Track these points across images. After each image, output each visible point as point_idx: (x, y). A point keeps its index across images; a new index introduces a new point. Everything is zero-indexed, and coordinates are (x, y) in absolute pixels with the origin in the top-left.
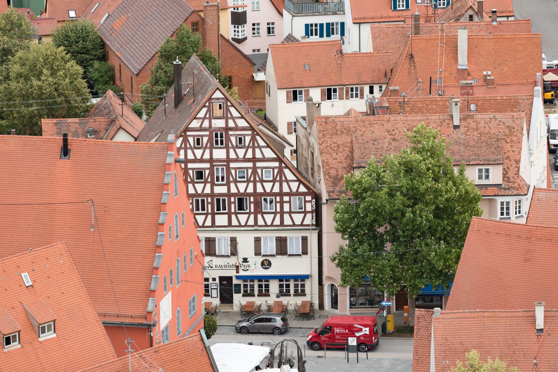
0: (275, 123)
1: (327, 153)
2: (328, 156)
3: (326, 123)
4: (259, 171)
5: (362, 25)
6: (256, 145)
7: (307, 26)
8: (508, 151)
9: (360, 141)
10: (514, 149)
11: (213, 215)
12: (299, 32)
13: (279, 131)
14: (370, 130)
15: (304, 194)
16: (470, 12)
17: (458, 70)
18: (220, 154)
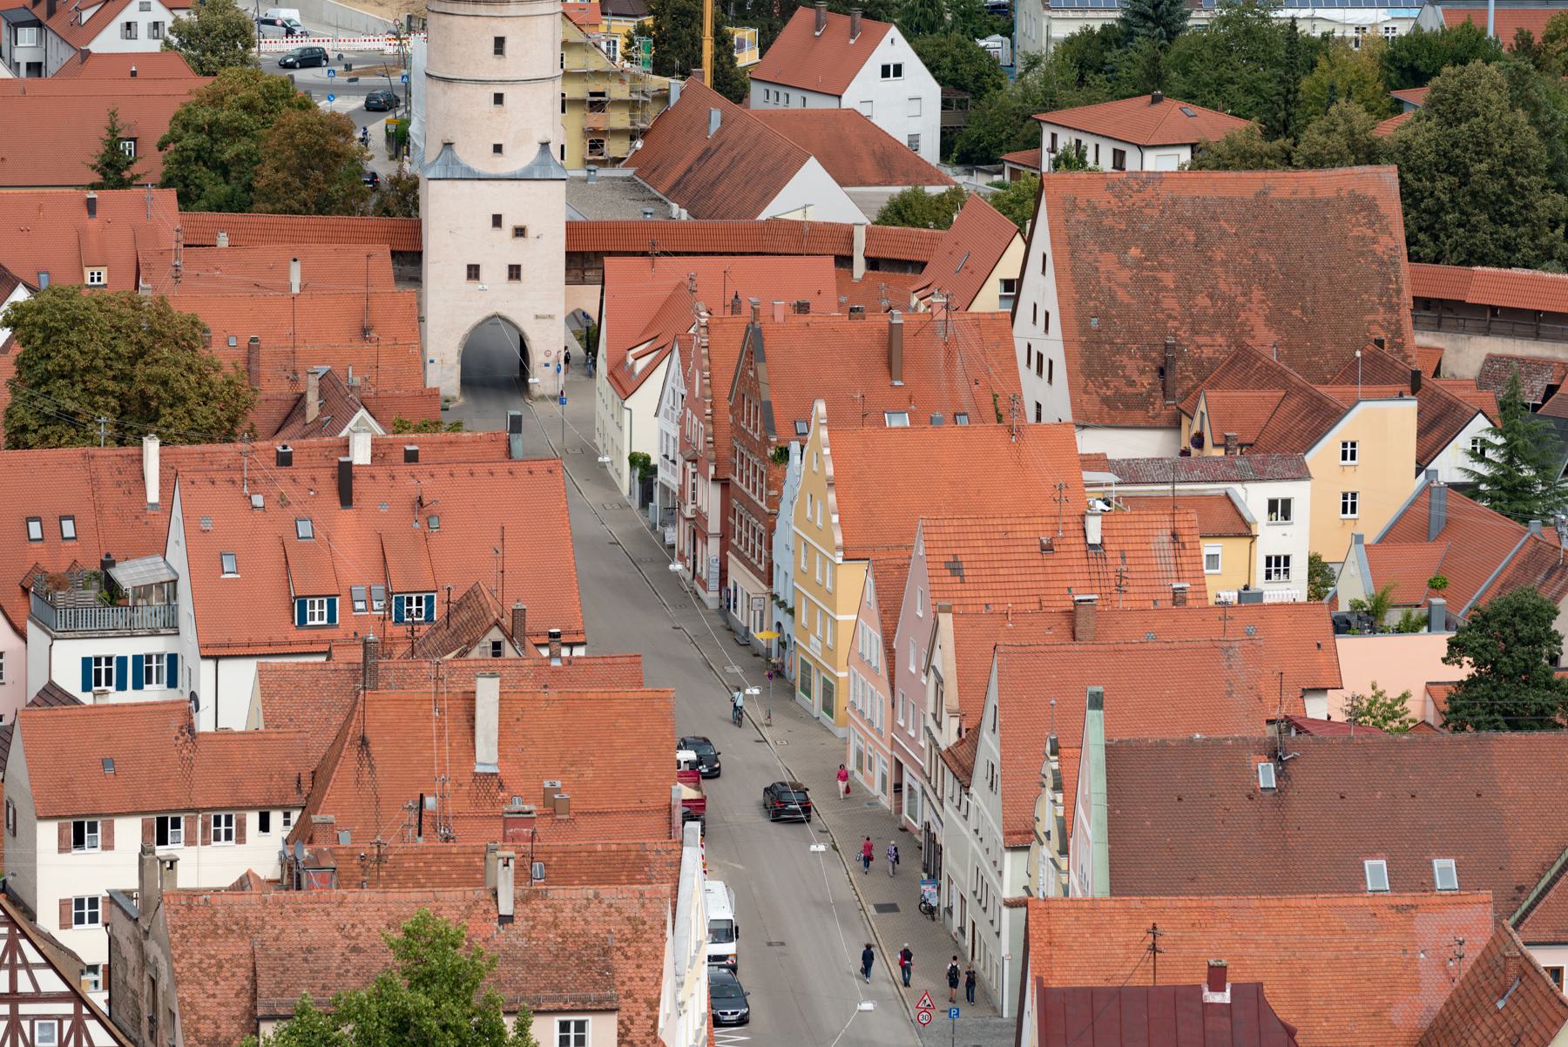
0: (27, 900)
1: (191, 983)
2: (195, 989)
3: (190, 907)
4: (25, 1025)
5: (221, 663)
6: (19, 961)
7: (86, 662)
8: (631, 979)
9: (273, 951)
10: (644, 972)
12: (69, 679)
13: (39, 921)
14: (296, 927)
16: (496, 635)
17: (476, 774)
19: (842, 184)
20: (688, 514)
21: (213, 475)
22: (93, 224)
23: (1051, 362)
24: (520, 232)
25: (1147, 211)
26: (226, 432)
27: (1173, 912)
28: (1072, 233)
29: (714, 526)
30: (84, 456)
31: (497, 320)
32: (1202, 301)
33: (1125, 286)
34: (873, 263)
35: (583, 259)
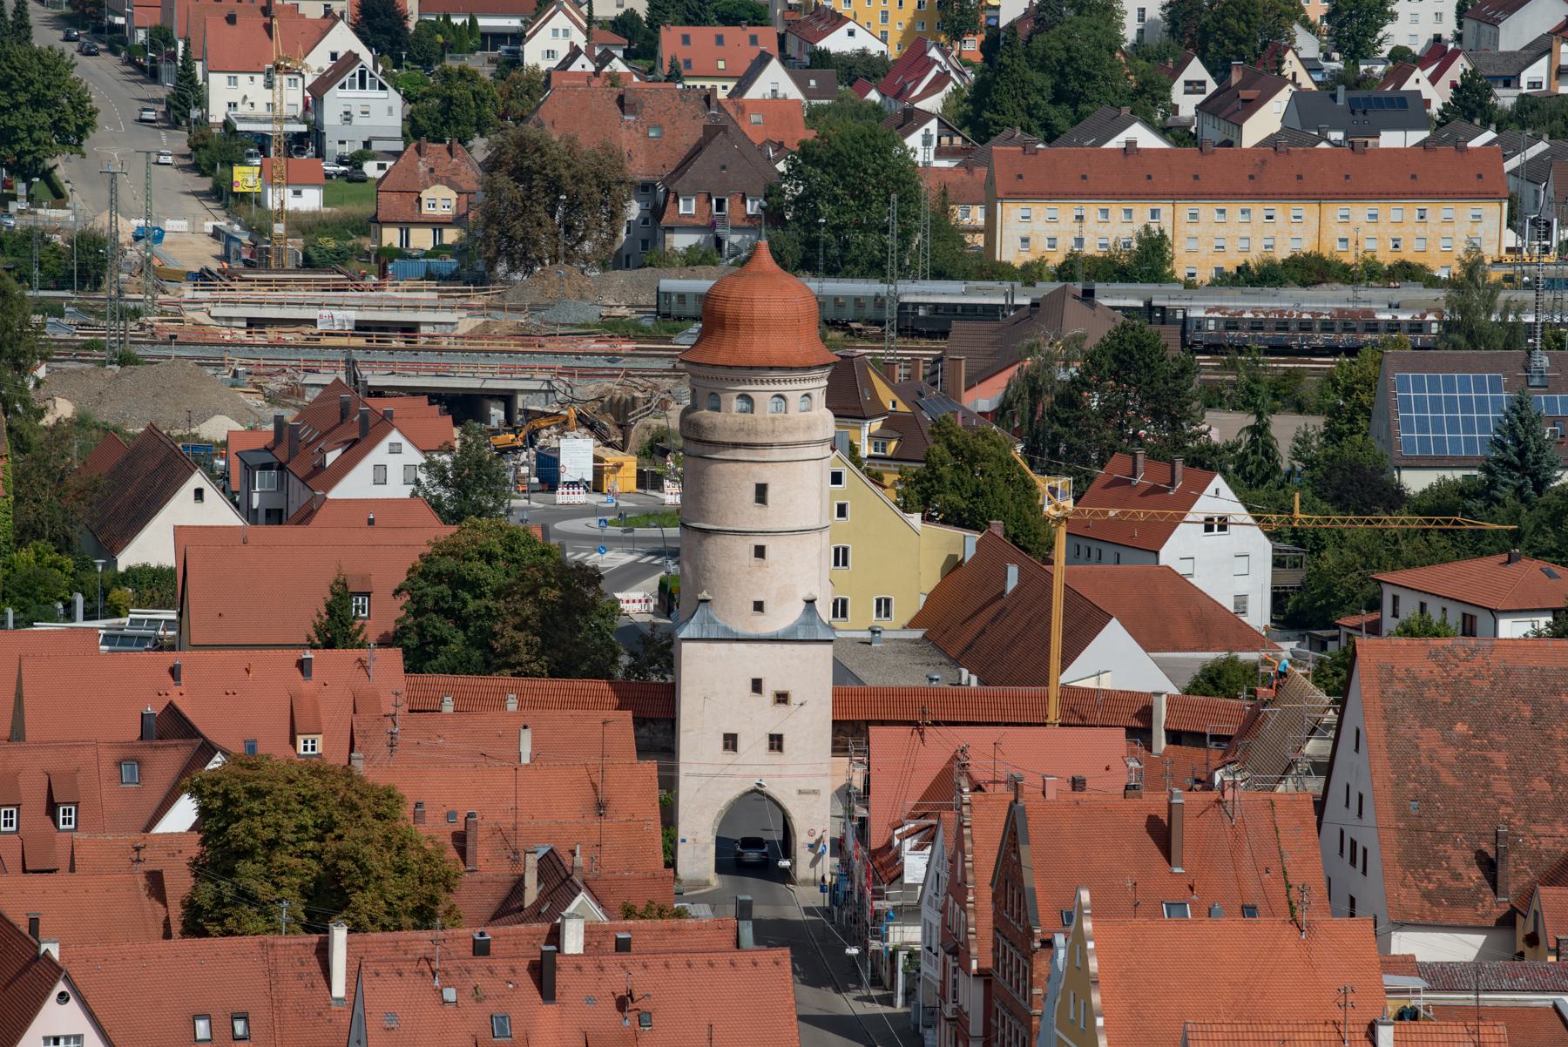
19: (1148, 648)
20: (949, 1014)
21: (400, 965)
22: (307, 686)
23: (1365, 851)
24: (782, 698)
25: (1476, 682)
26: (424, 916)
28: (1389, 706)
29: (976, 1026)
30: (262, 945)
31: (757, 795)
32: (1541, 785)
33: (1451, 766)
34: (1174, 737)
35: (849, 733)
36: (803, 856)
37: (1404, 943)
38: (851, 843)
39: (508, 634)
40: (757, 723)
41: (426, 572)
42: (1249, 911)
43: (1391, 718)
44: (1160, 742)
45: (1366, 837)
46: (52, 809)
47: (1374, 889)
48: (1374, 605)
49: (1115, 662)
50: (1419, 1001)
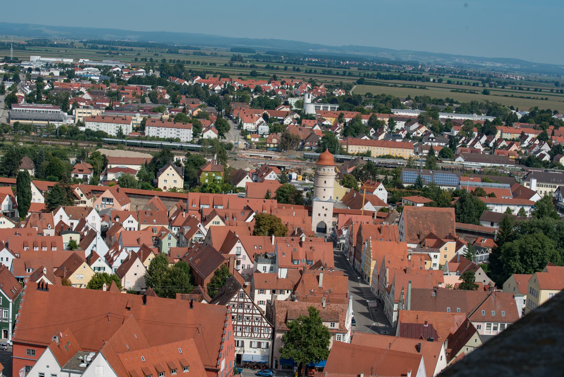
11: (237, 332)
15: (269, 327)
18: (241, 311)
22: (265, 204)
24: (326, 209)
26: (283, 235)
27: (420, 313)
29: (353, 254)
31: (322, 222)
32: (425, 226)
34: (377, 217)
35: (335, 214)
36: (328, 230)
37: (409, 245)
38: (335, 229)
39: (290, 199)
40: (323, 212)
41: (279, 190)
42: (390, 240)
43: (407, 216)
44: (375, 218)
45: (403, 231)
46: (233, 218)
47: (403, 238)
48: (401, 201)
49: (368, 207)
50: (412, 253)
